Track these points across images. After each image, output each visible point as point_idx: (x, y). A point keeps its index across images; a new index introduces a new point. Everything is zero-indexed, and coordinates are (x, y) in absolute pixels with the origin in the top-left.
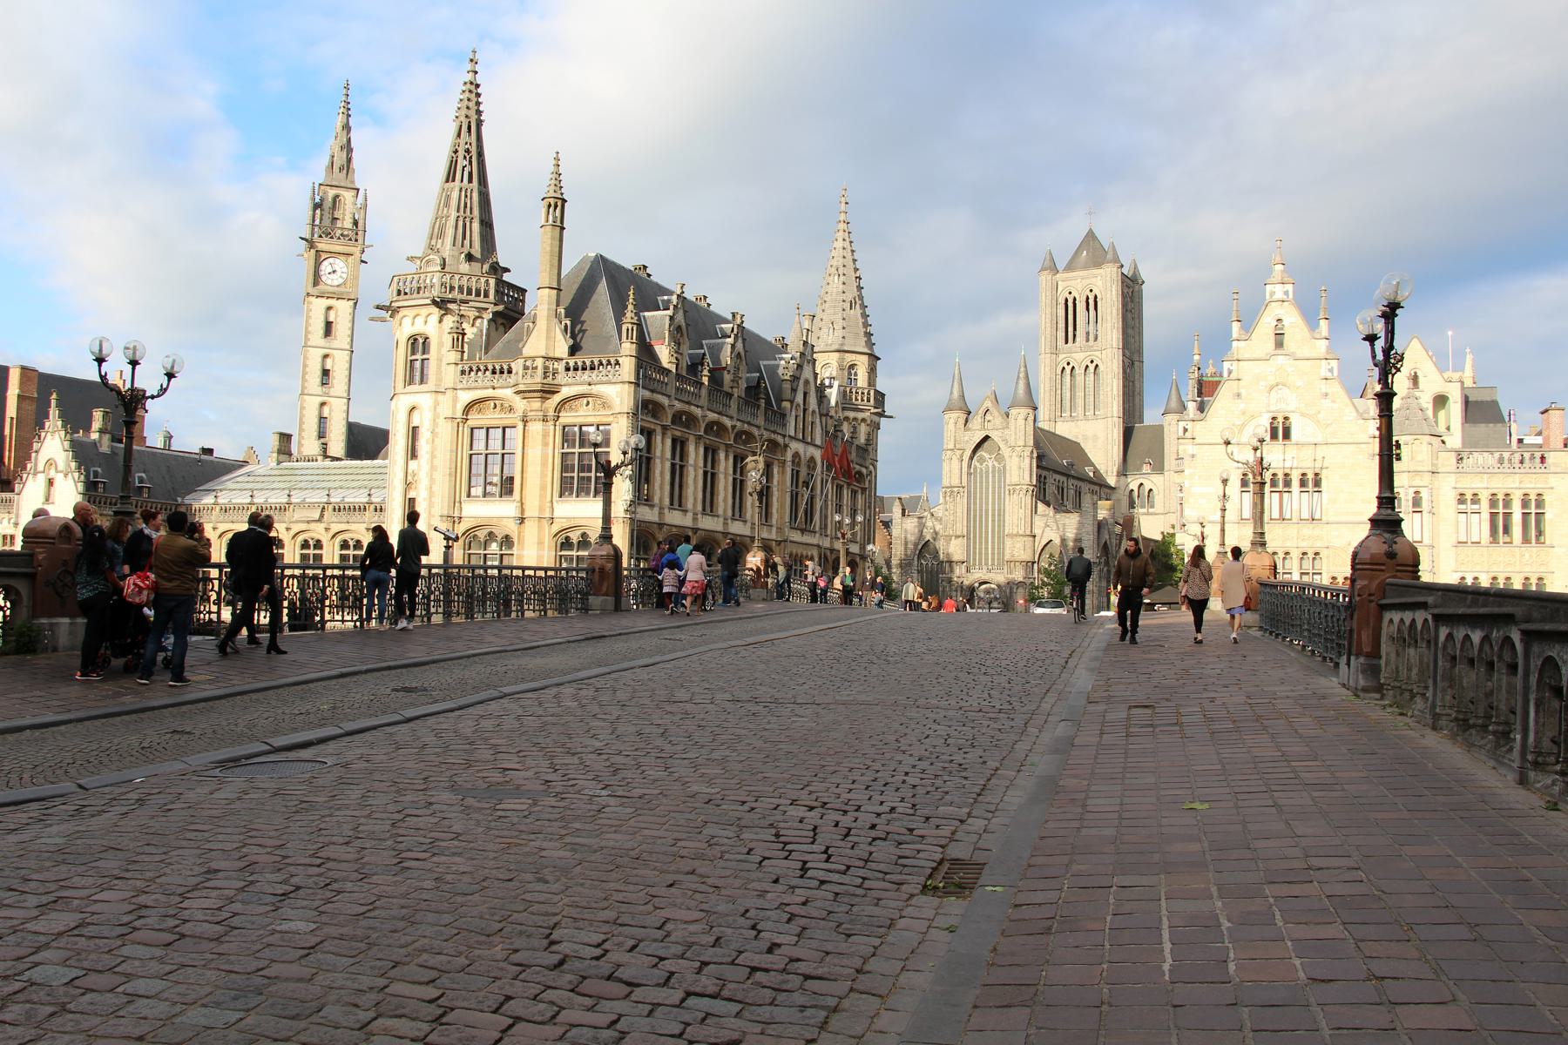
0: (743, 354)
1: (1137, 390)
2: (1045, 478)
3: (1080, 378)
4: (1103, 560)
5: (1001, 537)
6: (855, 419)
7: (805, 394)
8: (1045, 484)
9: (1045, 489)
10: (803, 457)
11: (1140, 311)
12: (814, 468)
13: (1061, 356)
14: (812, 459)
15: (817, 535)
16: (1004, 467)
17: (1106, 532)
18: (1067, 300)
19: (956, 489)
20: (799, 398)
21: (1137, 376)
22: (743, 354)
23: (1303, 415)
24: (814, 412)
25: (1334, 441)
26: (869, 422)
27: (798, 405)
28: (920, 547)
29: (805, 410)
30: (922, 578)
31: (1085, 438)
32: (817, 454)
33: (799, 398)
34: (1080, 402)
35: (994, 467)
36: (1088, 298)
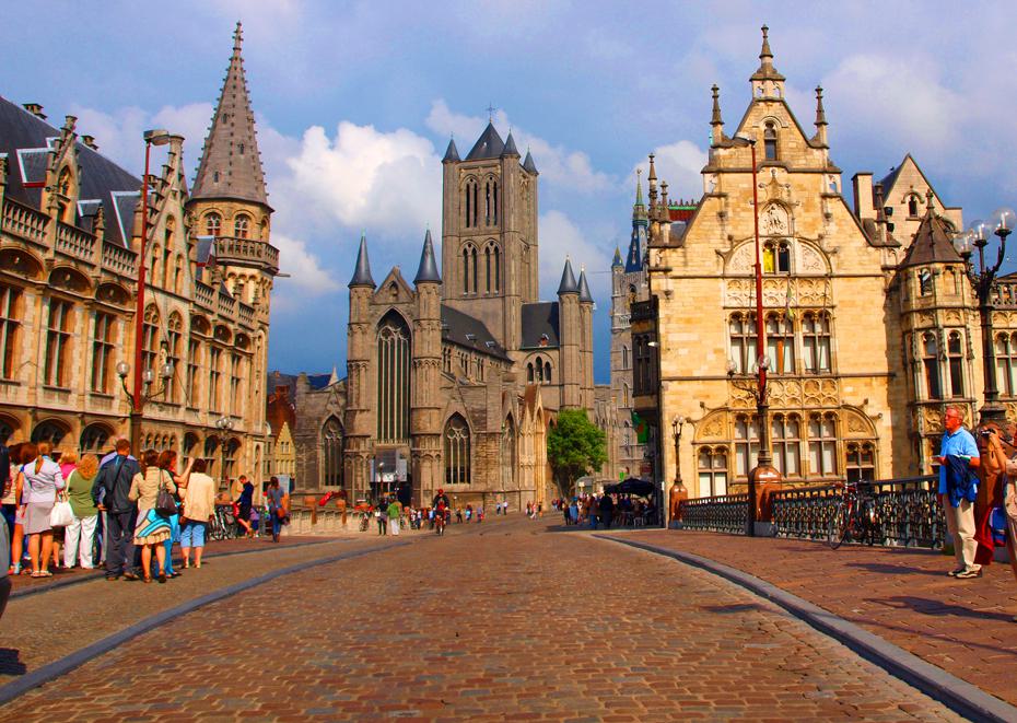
0: (73, 168)
1: (532, 271)
2: (450, 351)
3: (482, 260)
4: (507, 430)
5: (410, 411)
6: (243, 276)
7: (168, 233)
8: (449, 357)
9: (449, 362)
10: (162, 309)
11: (535, 200)
12: (179, 324)
13: (463, 239)
14: (176, 313)
15: (182, 409)
16: (410, 341)
17: (510, 403)
18: (468, 186)
19: (360, 363)
20: (160, 236)
21: (532, 259)
22: (73, 168)
23: (804, 240)
24: (180, 256)
25: (842, 272)
26: (259, 280)
27: (156, 246)
28: (324, 422)
29: (167, 253)
30: (326, 452)
31: (485, 314)
32: (186, 310)
33: (160, 236)
34: (482, 282)
35: (399, 340)
36: (488, 185)
